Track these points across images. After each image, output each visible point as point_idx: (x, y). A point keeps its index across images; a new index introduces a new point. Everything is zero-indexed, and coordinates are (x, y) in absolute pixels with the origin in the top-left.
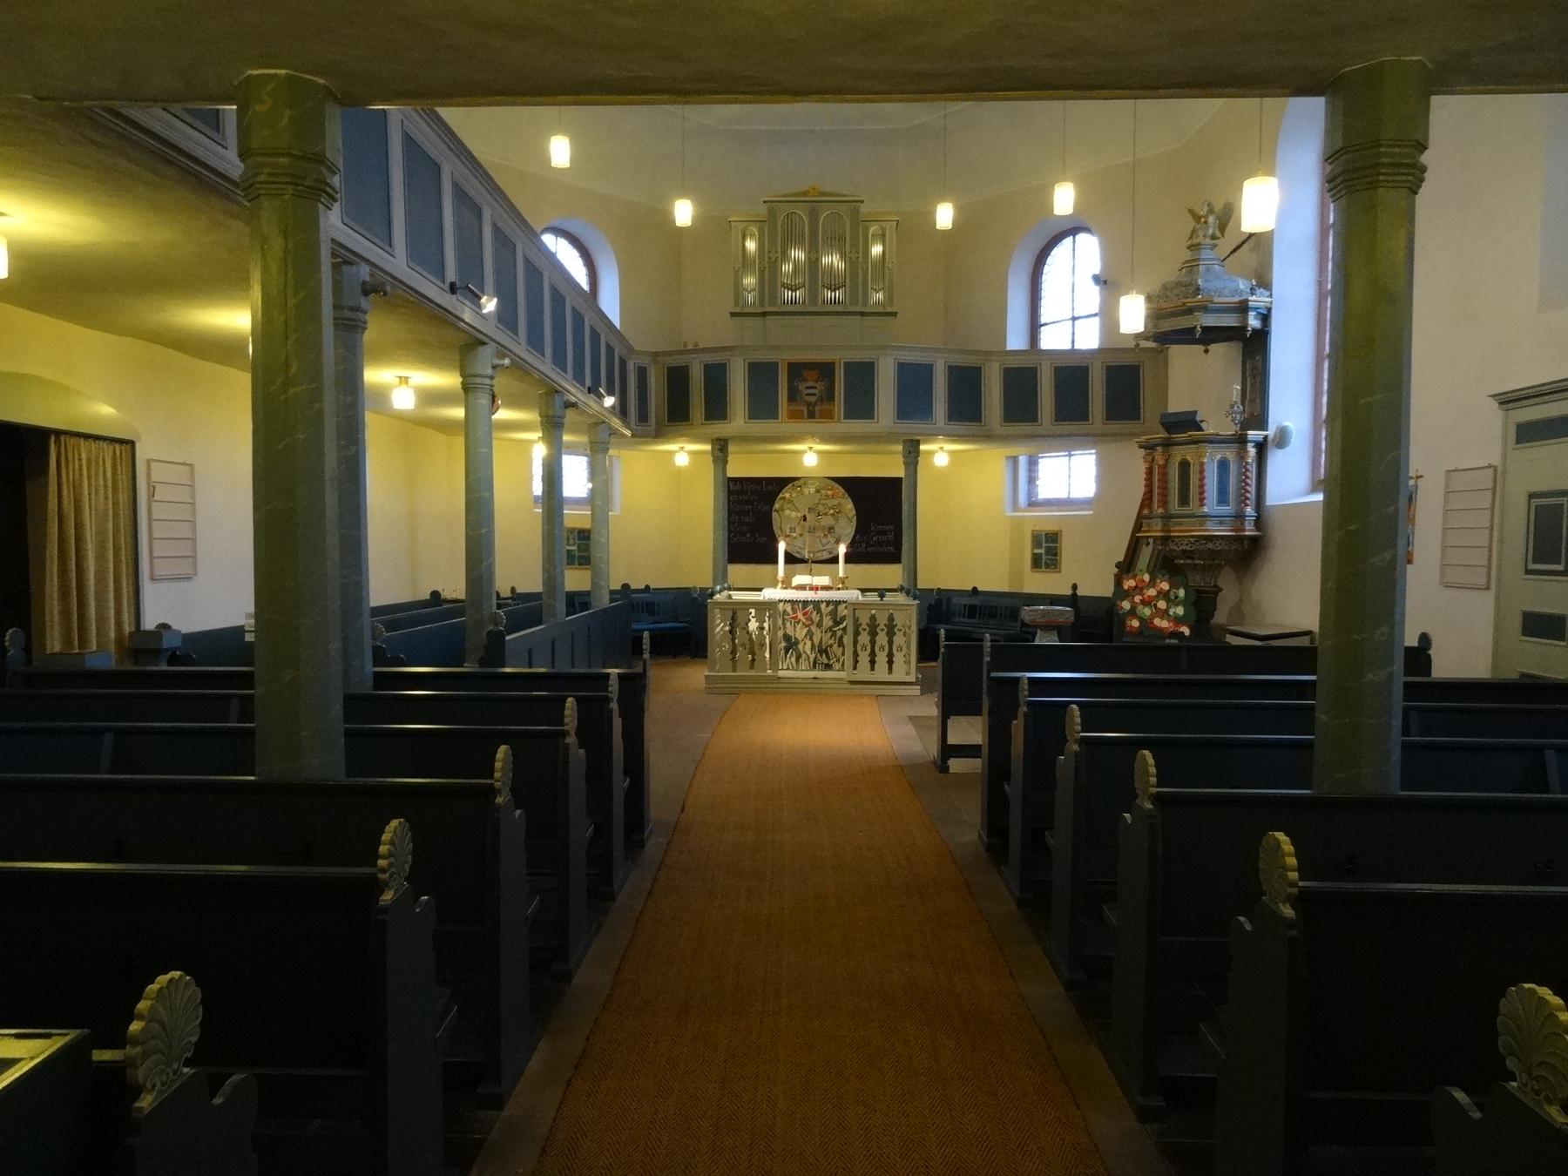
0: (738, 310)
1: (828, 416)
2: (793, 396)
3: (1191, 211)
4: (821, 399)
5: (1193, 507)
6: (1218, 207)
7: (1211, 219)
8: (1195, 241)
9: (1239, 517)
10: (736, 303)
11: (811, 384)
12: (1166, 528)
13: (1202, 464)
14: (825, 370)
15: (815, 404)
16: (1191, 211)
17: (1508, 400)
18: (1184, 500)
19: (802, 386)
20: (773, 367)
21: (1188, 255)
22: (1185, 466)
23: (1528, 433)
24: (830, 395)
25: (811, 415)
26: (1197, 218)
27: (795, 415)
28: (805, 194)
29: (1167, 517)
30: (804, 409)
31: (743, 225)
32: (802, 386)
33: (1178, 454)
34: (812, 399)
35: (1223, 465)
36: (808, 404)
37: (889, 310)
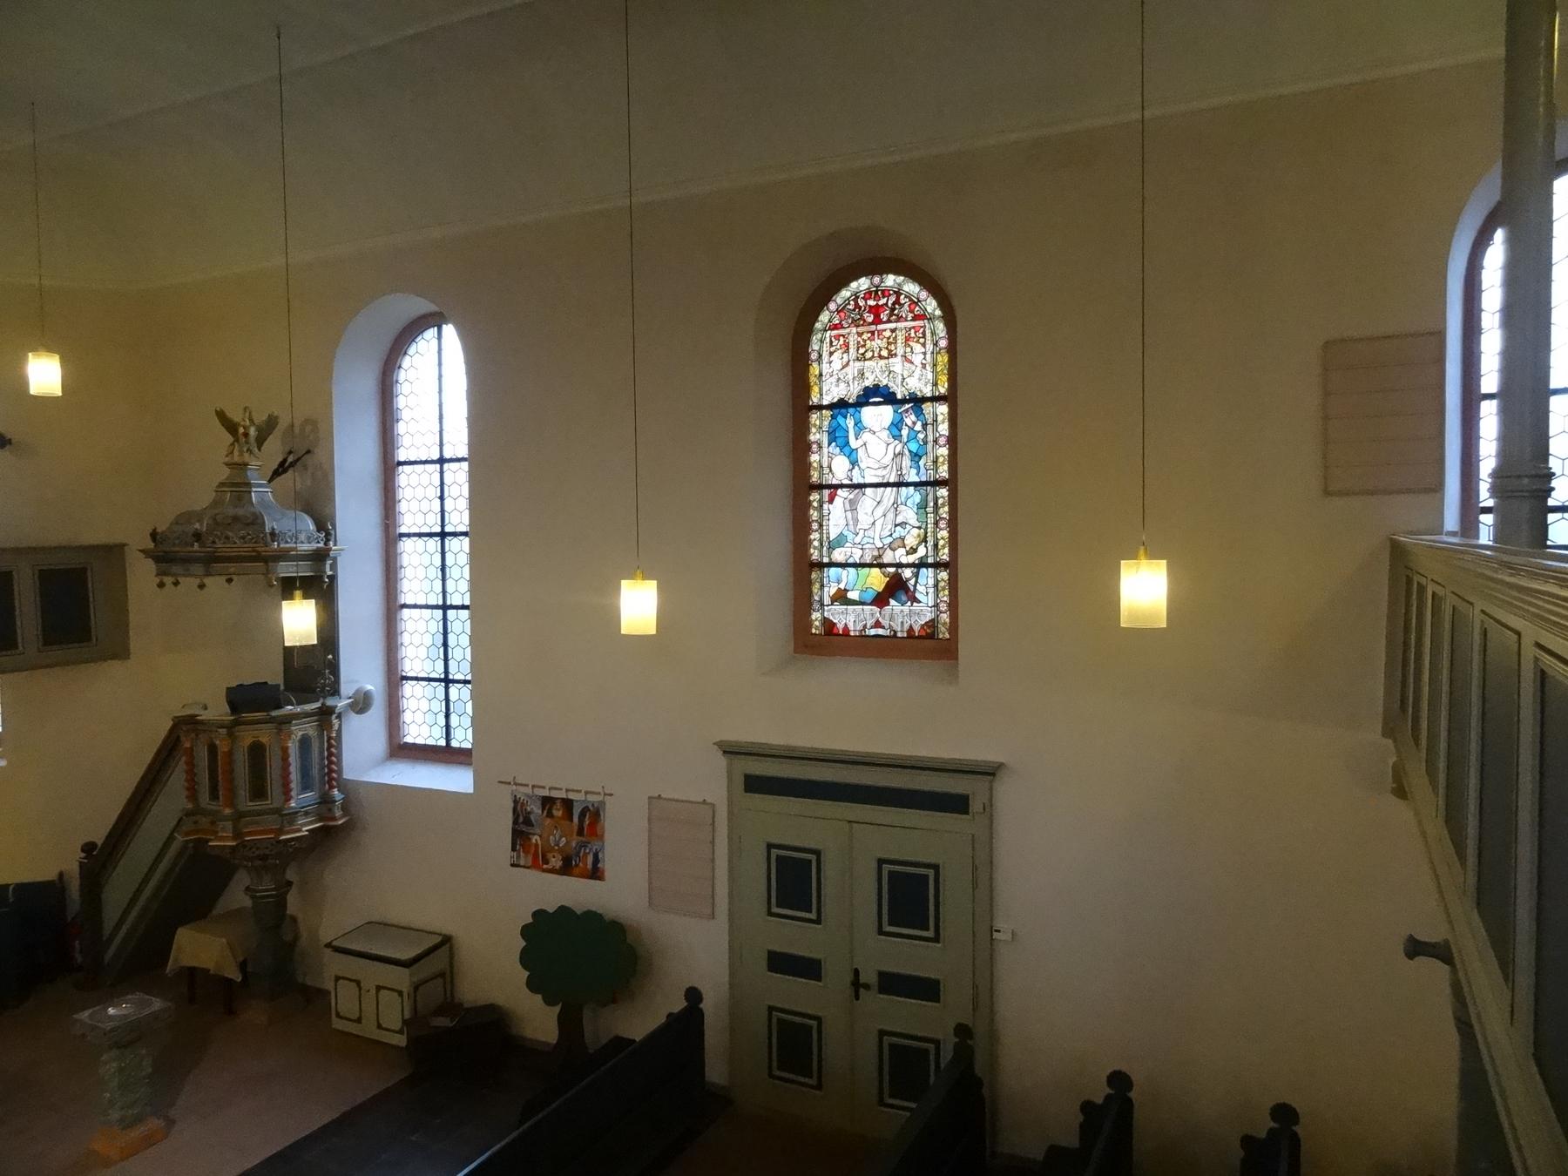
3: (221, 415)
5: (274, 801)
6: (261, 418)
7: (252, 431)
8: (236, 459)
9: (326, 800)
12: (237, 835)
13: (285, 750)
16: (221, 415)
17: (731, 751)
18: (259, 791)
21: (225, 473)
22: (257, 751)
23: (754, 784)
26: (231, 427)
29: (239, 816)
33: (247, 737)
35: (305, 742)
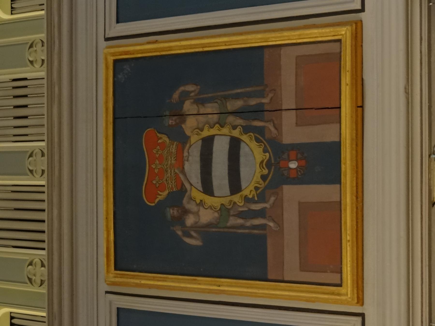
11: (193, 168)
15: (278, 151)
19: (203, 211)
24: (239, 72)
25: (323, 163)
30: (294, 194)
32: (203, 211)
36: (276, 178)
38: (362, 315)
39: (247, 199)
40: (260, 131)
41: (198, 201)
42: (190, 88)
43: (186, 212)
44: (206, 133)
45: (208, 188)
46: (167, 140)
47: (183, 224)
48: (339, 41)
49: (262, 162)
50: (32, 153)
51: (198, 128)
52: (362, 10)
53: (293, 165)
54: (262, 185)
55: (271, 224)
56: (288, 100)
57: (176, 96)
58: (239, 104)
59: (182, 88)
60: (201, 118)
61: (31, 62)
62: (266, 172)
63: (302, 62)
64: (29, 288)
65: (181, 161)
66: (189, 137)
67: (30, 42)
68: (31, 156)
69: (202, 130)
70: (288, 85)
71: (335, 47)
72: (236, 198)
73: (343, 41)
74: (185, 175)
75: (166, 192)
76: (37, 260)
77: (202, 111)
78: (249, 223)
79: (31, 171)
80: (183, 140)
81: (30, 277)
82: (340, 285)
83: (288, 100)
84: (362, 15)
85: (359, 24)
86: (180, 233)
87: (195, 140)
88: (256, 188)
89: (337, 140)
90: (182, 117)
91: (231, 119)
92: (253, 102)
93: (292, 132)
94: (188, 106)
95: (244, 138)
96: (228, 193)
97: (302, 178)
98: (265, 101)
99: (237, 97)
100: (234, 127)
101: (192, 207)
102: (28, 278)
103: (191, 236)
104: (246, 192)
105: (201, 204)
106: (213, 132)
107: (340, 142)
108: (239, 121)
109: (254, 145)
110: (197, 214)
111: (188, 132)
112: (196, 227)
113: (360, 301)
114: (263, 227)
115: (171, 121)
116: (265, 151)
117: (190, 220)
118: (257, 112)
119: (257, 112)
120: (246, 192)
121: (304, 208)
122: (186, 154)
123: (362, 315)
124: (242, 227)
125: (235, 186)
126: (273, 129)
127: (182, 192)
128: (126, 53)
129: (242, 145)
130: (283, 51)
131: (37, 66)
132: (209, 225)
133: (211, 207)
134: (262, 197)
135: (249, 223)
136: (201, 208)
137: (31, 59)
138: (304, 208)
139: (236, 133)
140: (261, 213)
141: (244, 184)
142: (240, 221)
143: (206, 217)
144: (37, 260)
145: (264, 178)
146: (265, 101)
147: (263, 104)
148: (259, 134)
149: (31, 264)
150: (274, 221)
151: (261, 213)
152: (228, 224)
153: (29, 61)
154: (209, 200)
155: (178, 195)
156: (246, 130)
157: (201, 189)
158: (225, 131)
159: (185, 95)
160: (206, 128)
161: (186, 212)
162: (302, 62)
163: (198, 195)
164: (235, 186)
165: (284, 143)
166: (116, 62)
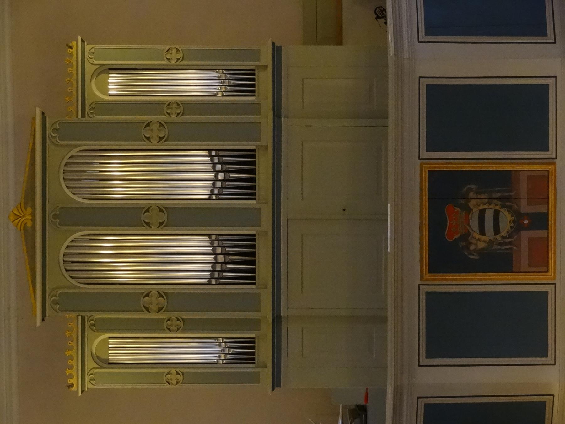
0: (267, 375)
1: (541, 185)
2: (499, 261)
4: (507, 201)
10: (254, 378)
11: (474, 224)
14: (444, 190)
15: (518, 216)
20: (436, 304)
25: (542, 221)
27: (541, 258)
28: (28, 234)
30: (525, 235)
31: (90, 364)
32: (480, 242)
34: (506, 218)
36: (517, 227)
37: (267, 58)
38: (555, 284)
39: (503, 237)
40: (511, 207)
41: (477, 238)
42: (473, 186)
43: (471, 244)
44: (482, 207)
45: (482, 231)
46: (460, 210)
47: (469, 249)
48: (548, 171)
49: (510, 221)
50: (149, 208)
51: (477, 205)
52: (556, 158)
53: (526, 222)
54: (510, 231)
55: (515, 248)
56: (524, 193)
57: (465, 189)
58: (498, 195)
59: (468, 186)
60: (478, 200)
61: (148, 138)
62: (512, 225)
63: (530, 178)
64: (147, 316)
65: (467, 219)
66: (472, 209)
67: (147, 122)
68: (147, 210)
69: (479, 206)
70: (523, 188)
71: (546, 173)
72: (498, 237)
73: (550, 171)
74: (470, 226)
75: (459, 235)
76: (154, 292)
77: (479, 197)
78: (504, 247)
79: (148, 224)
80: (469, 210)
81: (147, 306)
82: (547, 271)
83: (524, 193)
84: (555, 160)
85: (554, 164)
86: (466, 253)
87: (476, 211)
88: (508, 232)
89: (546, 211)
90: (468, 200)
91: (495, 201)
92: (506, 194)
93: (525, 207)
94: (471, 195)
95: (502, 210)
96: (493, 233)
97: (530, 227)
98: (512, 194)
99: (498, 192)
100: (496, 205)
101: (474, 241)
102: (144, 307)
103: (473, 255)
104: (502, 234)
105: (479, 239)
106: (485, 207)
107: (548, 213)
108: (499, 203)
109: (506, 213)
110: (476, 244)
111: (472, 207)
112: (475, 250)
113: (555, 279)
114: (511, 249)
115: (462, 201)
116: (512, 216)
117: (472, 247)
118: (509, 198)
119: (509, 198)
120: (502, 234)
121: (530, 240)
122: (470, 216)
123: (555, 284)
124: (500, 249)
125: (497, 231)
126: (516, 206)
127: (468, 234)
128: (436, 167)
129: (501, 213)
130: (521, 173)
131: (154, 141)
132: (483, 249)
133: (484, 241)
134: (510, 236)
135: (504, 247)
136: (479, 242)
137: (148, 136)
138: (530, 240)
139: (497, 208)
140: (510, 243)
141: (501, 230)
142: (499, 247)
143: (481, 245)
144: (154, 292)
145: (511, 227)
146: (512, 194)
147: (511, 196)
148: (509, 209)
149: (147, 295)
150: (516, 246)
151: (510, 243)
152: (493, 248)
153: (145, 137)
154: (483, 238)
155: (466, 236)
156: (502, 207)
157: (478, 232)
158: (491, 206)
159: (471, 189)
160: (481, 205)
161: (471, 244)
162: (530, 178)
163: (477, 236)
164: (497, 231)
165: (522, 212)
166: (429, 171)
